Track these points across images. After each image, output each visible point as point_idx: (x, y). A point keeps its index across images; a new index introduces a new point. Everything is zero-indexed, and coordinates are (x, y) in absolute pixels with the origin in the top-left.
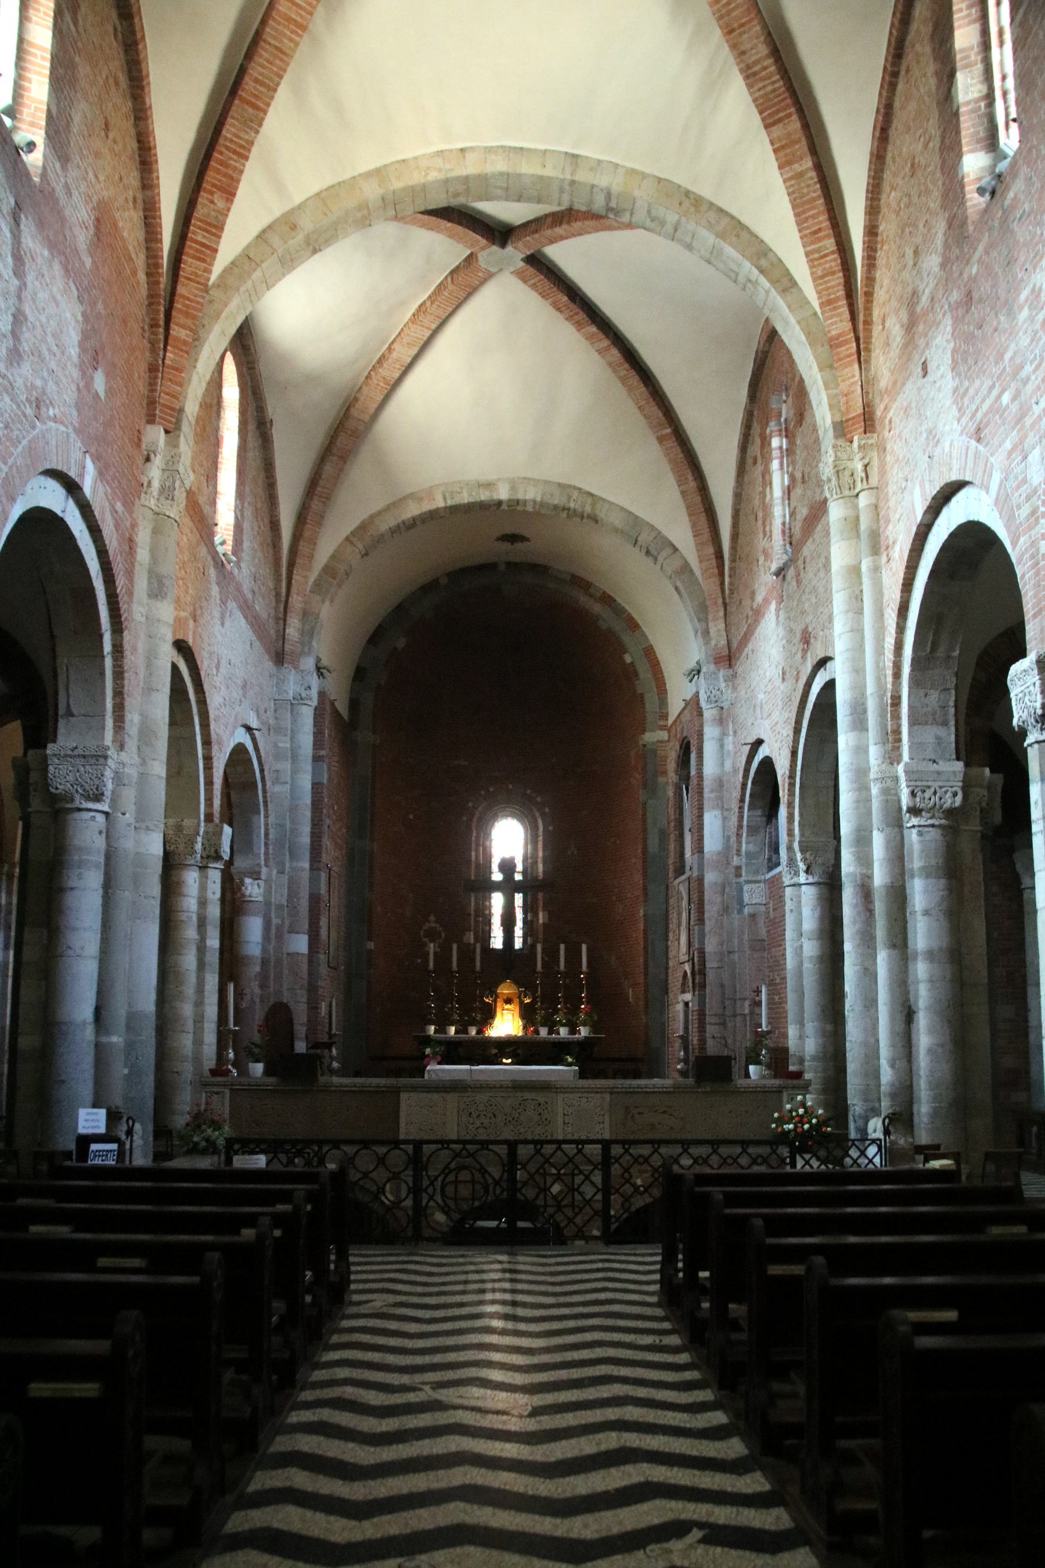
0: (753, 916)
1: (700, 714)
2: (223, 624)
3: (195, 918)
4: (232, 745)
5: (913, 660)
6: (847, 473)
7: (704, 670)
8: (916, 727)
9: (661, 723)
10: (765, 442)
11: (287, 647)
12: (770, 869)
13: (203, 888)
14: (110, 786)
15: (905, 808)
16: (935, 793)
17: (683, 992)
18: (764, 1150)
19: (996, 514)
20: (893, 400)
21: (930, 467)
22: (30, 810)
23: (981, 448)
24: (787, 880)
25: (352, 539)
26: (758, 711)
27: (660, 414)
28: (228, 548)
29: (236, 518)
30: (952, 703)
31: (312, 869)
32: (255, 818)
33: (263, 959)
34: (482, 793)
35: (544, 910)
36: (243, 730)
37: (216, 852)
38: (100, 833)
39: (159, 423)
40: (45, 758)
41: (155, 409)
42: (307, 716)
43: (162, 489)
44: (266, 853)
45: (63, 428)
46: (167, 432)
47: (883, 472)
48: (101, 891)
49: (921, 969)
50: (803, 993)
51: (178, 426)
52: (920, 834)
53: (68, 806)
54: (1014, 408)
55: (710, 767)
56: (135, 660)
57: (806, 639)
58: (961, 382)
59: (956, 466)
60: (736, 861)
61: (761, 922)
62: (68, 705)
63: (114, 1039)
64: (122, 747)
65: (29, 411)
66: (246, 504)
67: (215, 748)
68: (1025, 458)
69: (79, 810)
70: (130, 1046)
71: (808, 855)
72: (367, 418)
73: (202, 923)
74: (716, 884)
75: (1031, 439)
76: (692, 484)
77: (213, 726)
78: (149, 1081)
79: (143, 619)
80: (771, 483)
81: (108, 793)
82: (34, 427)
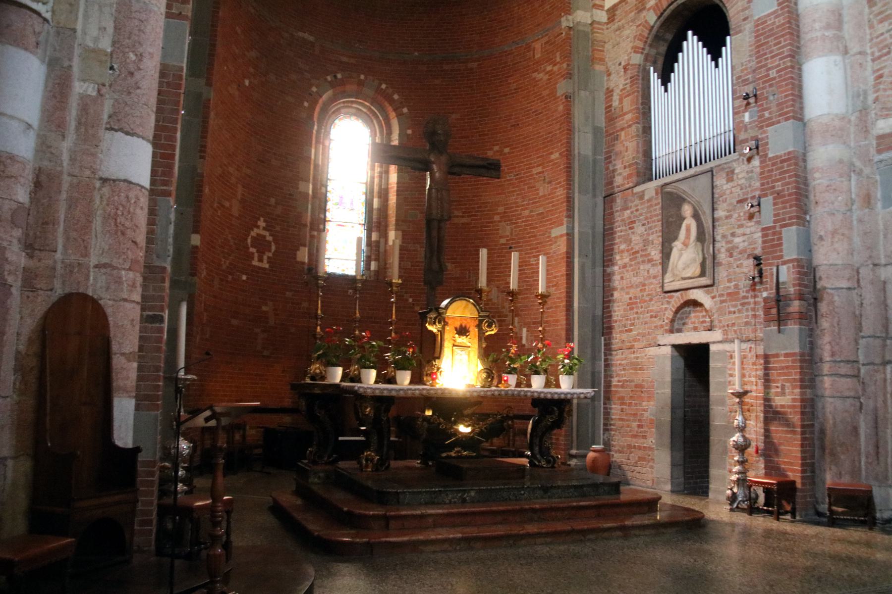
33: (39, 173)
34: (329, 78)
35: (396, 230)
74: (841, 161)
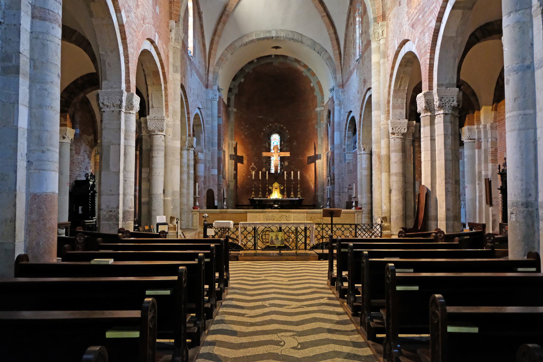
0: (349, 163)
1: (334, 103)
2: (191, 78)
3: (186, 165)
4: (195, 114)
5: (394, 90)
6: (377, 33)
7: (335, 89)
8: (394, 110)
9: (322, 105)
10: (354, 19)
11: (209, 83)
12: (354, 149)
13: (188, 155)
14: (165, 128)
15: (390, 133)
16: (399, 128)
17: (328, 186)
18: (348, 226)
19: (416, 50)
20: (391, 12)
21: (400, 34)
22: (142, 135)
23: (413, 30)
24: (358, 153)
25: (228, 49)
26: (351, 102)
27: (322, 9)
28: (192, 54)
29: (194, 44)
30: (405, 103)
31: (218, 150)
32: (201, 135)
34: (268, 126)
36: (198, 109)
37: (192, 145)
38: (163, 141)
39: (174, 20)
40: (146, 120)
41: (172, 15)
42: (216, 103)
43: (175, 39)
44: (205, 145)
45: (150, 25)
46: (176, 22)
47: (387, 34)
48: (164, 158)
49: (394, 178)
50: (362, 186)
51: (179, 21)
52: (394, 140)
53: (154, 133)
54: (422, 20)
55: (336, 119)
56: (170, 91)
57: (365, 82)
58: (409, 9)
59: (407, 35)
60: (344, 147)
61: (351, 165)
62: (152, 105)
63: (169, 198)
64: (168, 117)
65: (142, 22)
66: (196, 39)
67: (190, 114)
68: (424, 35)
69: (157, 134)
70: (173, 200)
71: (364, 145)
72: (231, 11)
73: (188, 166)
75: (426, 30)
76: (332, 31)
77: (190, 108)
78: (179, 210)
79: (172, 79)
80: (356, 32)
81: (165, 130)
82: (143, 27)
